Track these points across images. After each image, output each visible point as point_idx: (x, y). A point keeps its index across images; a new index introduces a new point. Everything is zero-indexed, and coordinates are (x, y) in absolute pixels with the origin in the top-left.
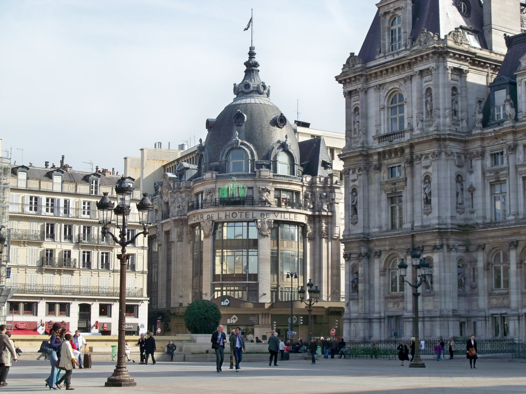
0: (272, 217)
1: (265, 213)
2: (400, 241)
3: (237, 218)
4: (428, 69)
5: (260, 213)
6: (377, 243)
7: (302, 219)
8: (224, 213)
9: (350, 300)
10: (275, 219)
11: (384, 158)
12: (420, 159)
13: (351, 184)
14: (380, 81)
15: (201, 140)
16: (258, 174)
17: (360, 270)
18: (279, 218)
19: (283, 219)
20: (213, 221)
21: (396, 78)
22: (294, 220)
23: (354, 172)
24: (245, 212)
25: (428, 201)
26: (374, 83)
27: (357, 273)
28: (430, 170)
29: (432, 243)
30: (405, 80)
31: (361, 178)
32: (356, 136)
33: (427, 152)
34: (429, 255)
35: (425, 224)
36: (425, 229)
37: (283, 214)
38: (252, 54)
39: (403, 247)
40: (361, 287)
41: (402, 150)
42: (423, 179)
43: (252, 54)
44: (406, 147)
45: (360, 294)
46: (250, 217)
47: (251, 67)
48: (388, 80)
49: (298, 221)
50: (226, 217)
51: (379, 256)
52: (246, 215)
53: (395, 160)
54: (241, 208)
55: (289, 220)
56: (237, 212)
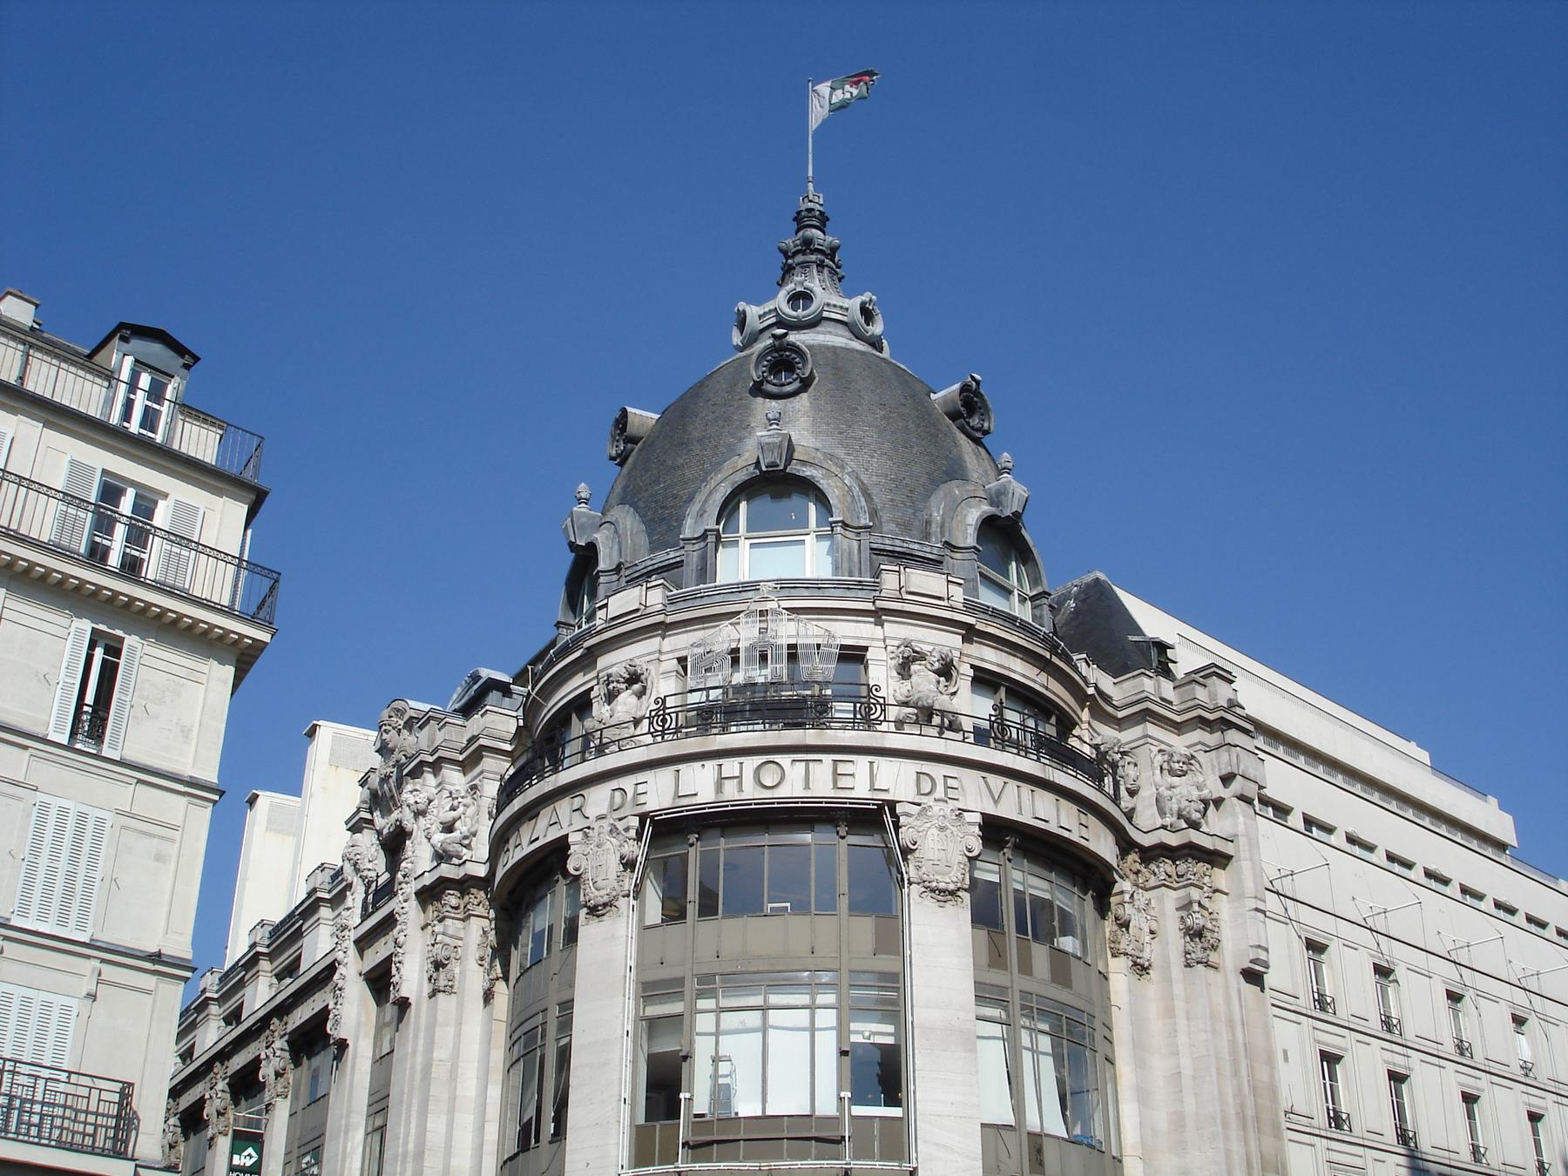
0: (979, 796)
3: (783, 792)
5: (911, 767)
7: (1103, 845)
8: (711, 765)
10: (992, 810)
16: (889, 581)
19: (1026, 819)
20: (643, 818)
22: (1074, 837)
24: (828, 759)
49: (1092, 846)
50: (719, 788)
52: (836, 774)
54: (810, 736)
55: (1052, 828)
56: (784, 760)
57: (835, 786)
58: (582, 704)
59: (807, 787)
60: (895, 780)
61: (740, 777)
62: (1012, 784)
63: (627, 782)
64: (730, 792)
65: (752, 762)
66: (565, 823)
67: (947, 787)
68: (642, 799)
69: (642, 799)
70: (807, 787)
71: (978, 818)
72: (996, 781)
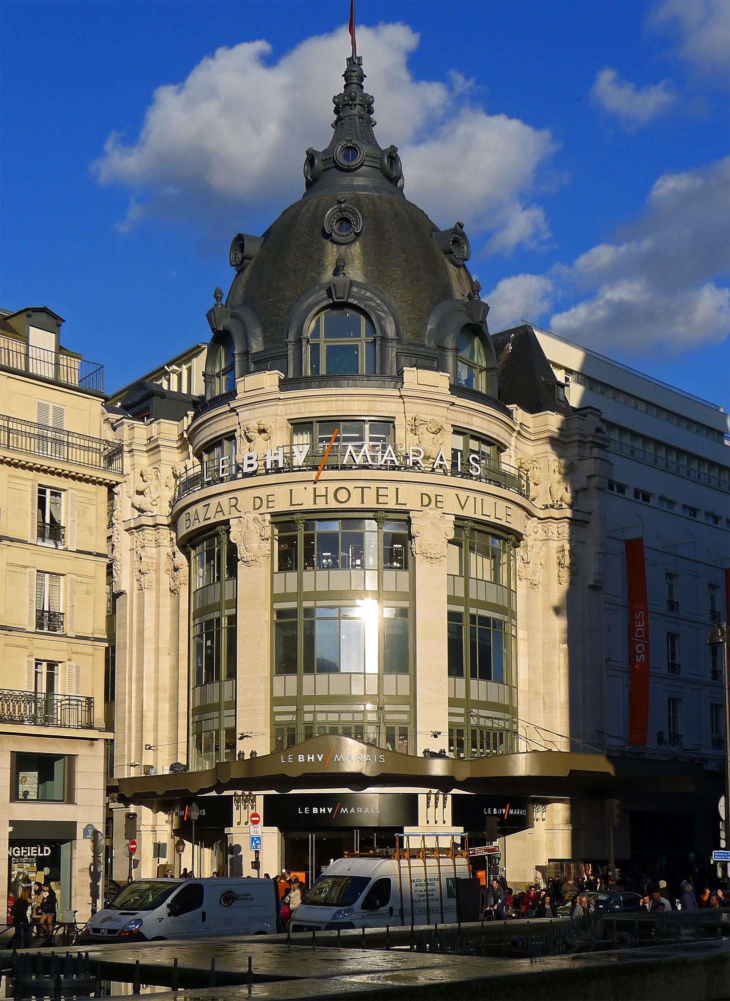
1: (432, 491)
15: (218, 296)
18: (468, 512)
24: (374, 485)
37: (479, 497)
46: (392, 505)
52: (378, 495)
56: (350, 485)
57: (378, 503)
58: (230, 437)
59: (363, 502)
60: (409, 497)
61: (326, 496)
62: (472, 495)
63: (262, 492)
64: (321, 504)
65: (333, 486)
66: (226, 511)
67: (436, 501)
68: (270, 504)
69: (270, 504)
70: (363, 502)
71: (453, 518)
72: (463, 495)
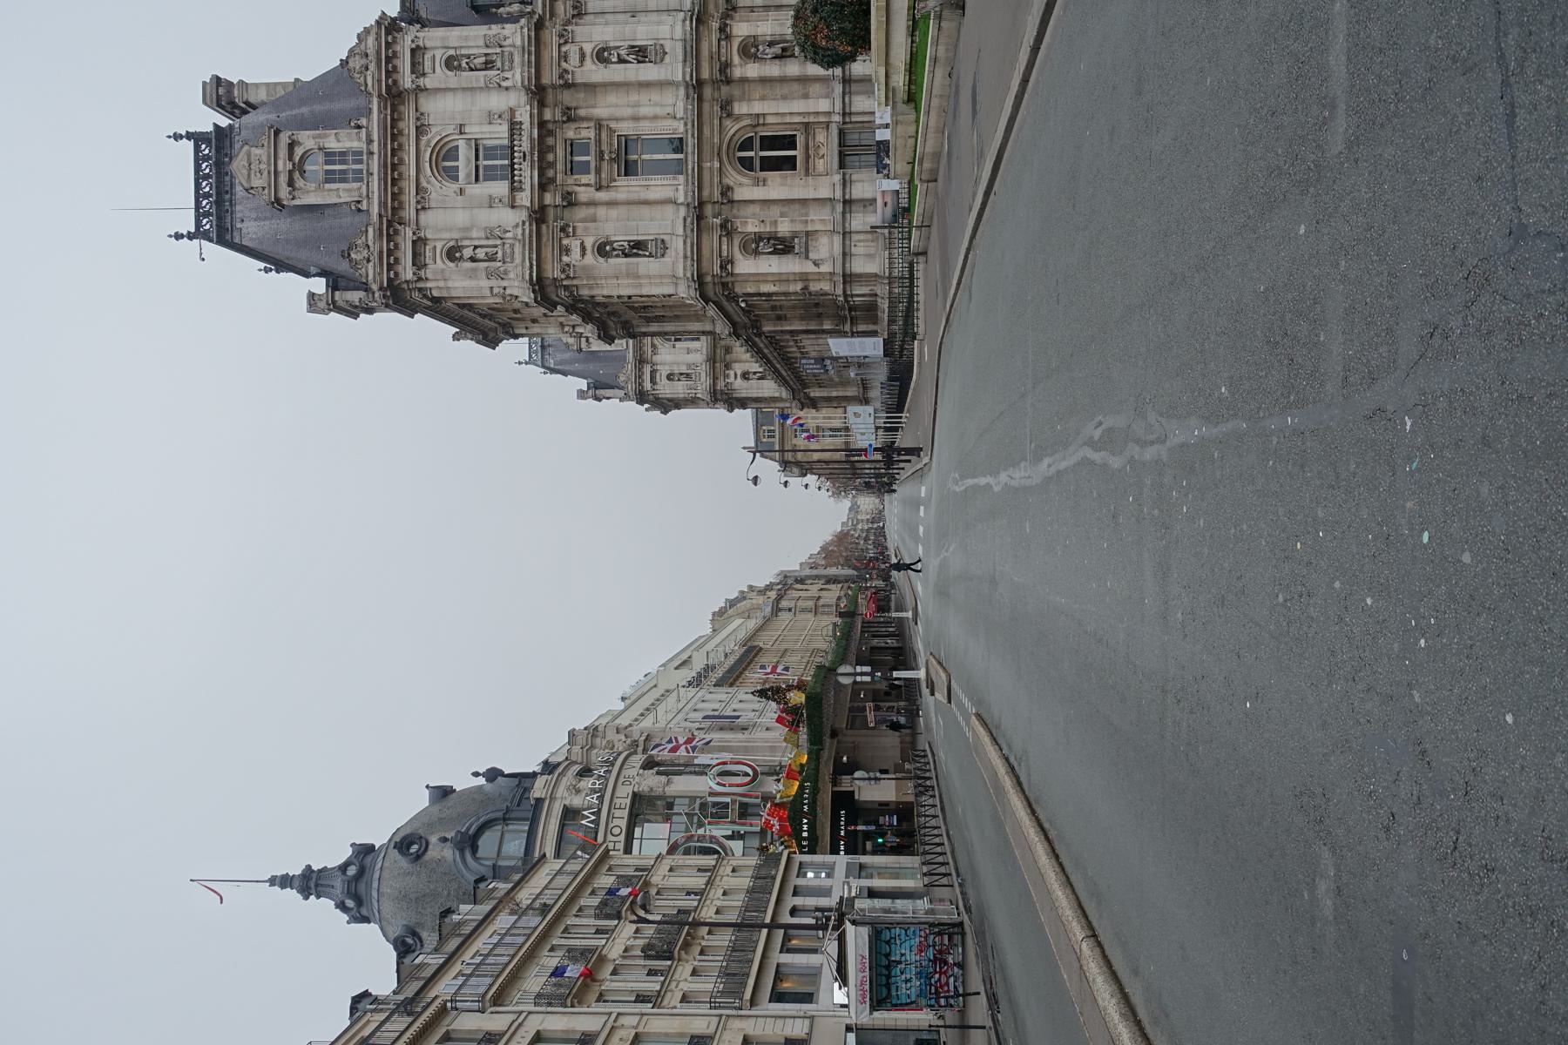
2: (707, 131)
4: (413, 51)
6: (706, 193)
9: (807, 257)
11: (553, 180)
12: (566, 71)
13: (590, 259)
14: (410, 198)
17: (752, 227)
21: (413, 150)
23: (567, 251)
25: (640, 54)
26: (409, 212)
27: (759, 238)
28: (588, 48)
29: (715, 36)
30: (420, 130)
31: (579, 232)
32: (500, 255)
33: (555, 54)
34: (735, 48)
35: (681, 58)
36: (693, 53)
38: (284, 881)
39: (716, 122)
40: (784, 228)
41: (542, 124)
42: (601, 66)
43: (284, 881)
44: (540, 114)
45: (799, 227)
47: (310, 883)
48: (413, 173)
51: (729, 188)
53: (560, 152)
